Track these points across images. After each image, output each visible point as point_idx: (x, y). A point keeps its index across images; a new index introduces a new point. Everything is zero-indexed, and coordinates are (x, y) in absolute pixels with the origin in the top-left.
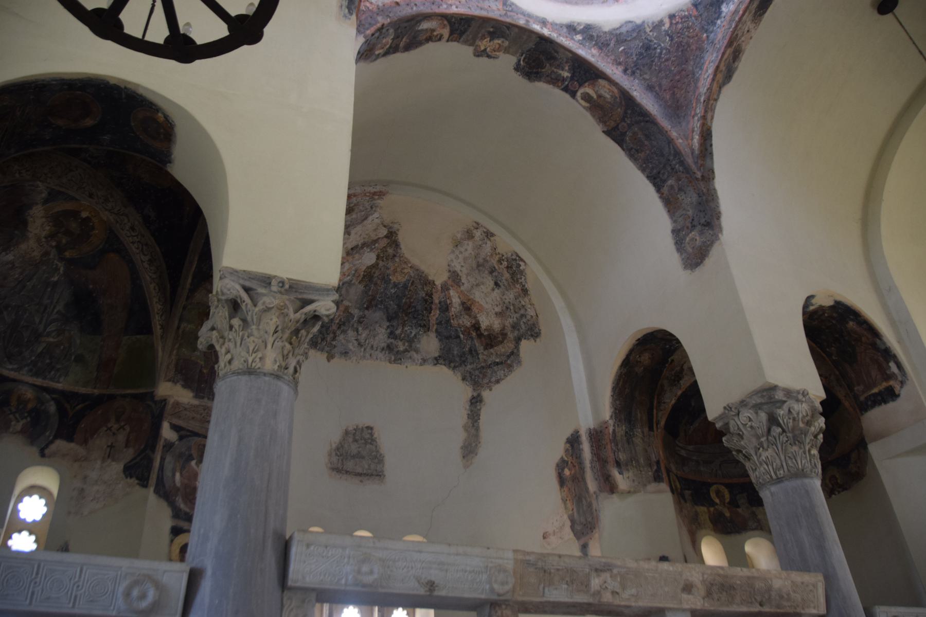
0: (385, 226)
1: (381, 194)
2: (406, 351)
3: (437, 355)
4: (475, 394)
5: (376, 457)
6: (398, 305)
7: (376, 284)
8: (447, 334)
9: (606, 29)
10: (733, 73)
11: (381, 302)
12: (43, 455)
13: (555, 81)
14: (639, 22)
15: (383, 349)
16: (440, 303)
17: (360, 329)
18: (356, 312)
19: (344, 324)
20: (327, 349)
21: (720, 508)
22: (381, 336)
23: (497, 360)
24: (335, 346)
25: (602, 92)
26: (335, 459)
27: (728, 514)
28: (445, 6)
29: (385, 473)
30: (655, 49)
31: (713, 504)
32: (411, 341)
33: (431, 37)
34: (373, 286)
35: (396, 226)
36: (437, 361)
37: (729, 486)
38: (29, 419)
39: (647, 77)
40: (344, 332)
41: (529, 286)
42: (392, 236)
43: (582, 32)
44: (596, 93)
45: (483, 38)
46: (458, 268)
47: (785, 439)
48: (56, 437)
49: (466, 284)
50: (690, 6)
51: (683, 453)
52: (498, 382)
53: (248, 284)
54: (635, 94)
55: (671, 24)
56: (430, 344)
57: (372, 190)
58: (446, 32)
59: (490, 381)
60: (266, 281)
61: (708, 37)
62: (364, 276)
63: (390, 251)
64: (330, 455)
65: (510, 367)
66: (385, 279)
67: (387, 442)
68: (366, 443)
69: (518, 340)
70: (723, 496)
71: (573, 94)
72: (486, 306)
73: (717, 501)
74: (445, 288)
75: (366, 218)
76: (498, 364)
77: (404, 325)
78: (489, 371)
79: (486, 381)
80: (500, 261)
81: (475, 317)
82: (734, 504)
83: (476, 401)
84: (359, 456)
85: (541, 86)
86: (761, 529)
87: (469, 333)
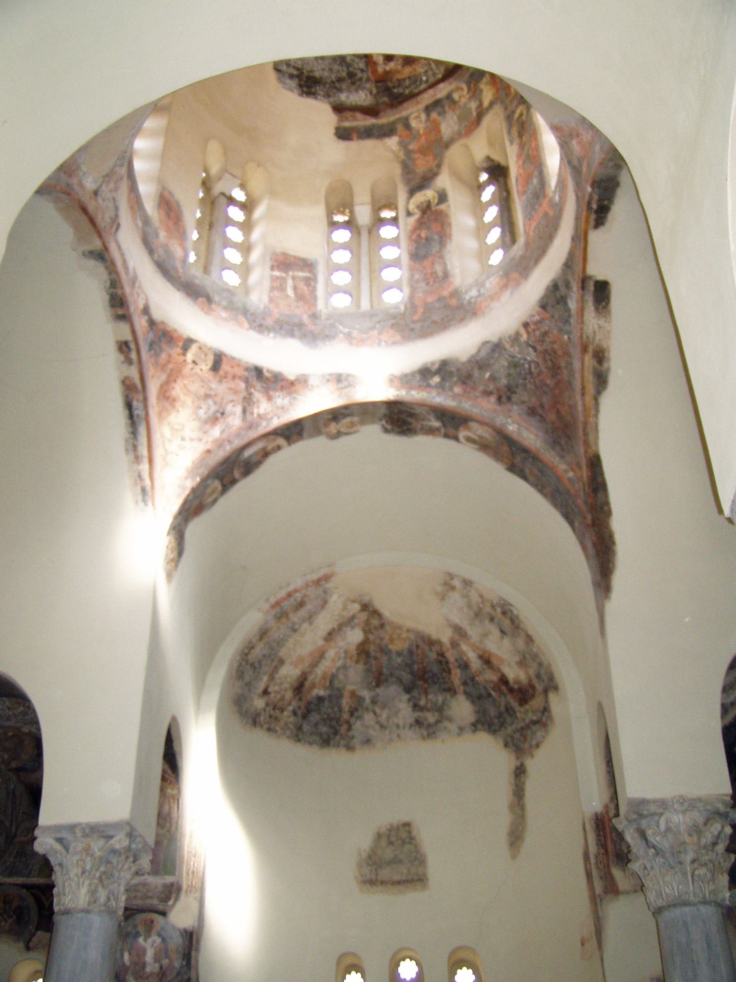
0: (354, 601)
1: (327, 578)
2: (438, 722)
3: (473, 719)
4: (519, 764)
5: (416, 858)
6: (412, 673)
7: (376, 658)
8: (478, 697)
9: (464, 358)
10: (606, 377)
11: (391, 675)
12: (28, 948)
13: (431, 431)
14: (495, 339)
15: (411, 726)
16: (456, 660)
17: (378, 710)
18: (366, 694)
19: (356, 709)
20: (342, 742)
22: (404, 711)
23: (535, 718)
24: (353, 737)
25: (480, 432)
26: (366, 870)
28: (264, 424)
29: (430, 876)
30: (523, 365)
32: (440, 709)
33: (265, 454)
34: (373, 662)
35: (366, 599)
36: (475, 726)
38: (14, 917)
39: (525, 398)
40: (359, 718)
41: (531, 632)
42: (365, 607)
43: (438, 372)
44: (475, 434)
45: (326, 425)
46: (457, 621)
47: (662, 860)
48: (37, 929)
49: (474, 633)
50: (539, 309)
52: (538, 746)
53: (59, 835)
54: (512, 428)
55: (528, 333)
56: (462, 709)
57: (315, 577)
58: (281, 441)
59: (531, 746)
60: (72, 828)
61: (569, 338)
62: (359, 654)
63: (375, 622)
64: (360, 866)
65: (545, 725)
66: (384, 650)
67: (429, 838)
68: (404, 842)
69: (546, 691)
71: (456, 439)
72: (504, 656)
74: (454, 645)
75: (325, 602)
76: (535, 723)
77: (426, 694)
78: (529, 732)
79: (527, 746)
80: (493, 607)
81: (499, 670)
83: (520, 772)
84: (395, 861)
85: (420, 440)
87: (500, 689)
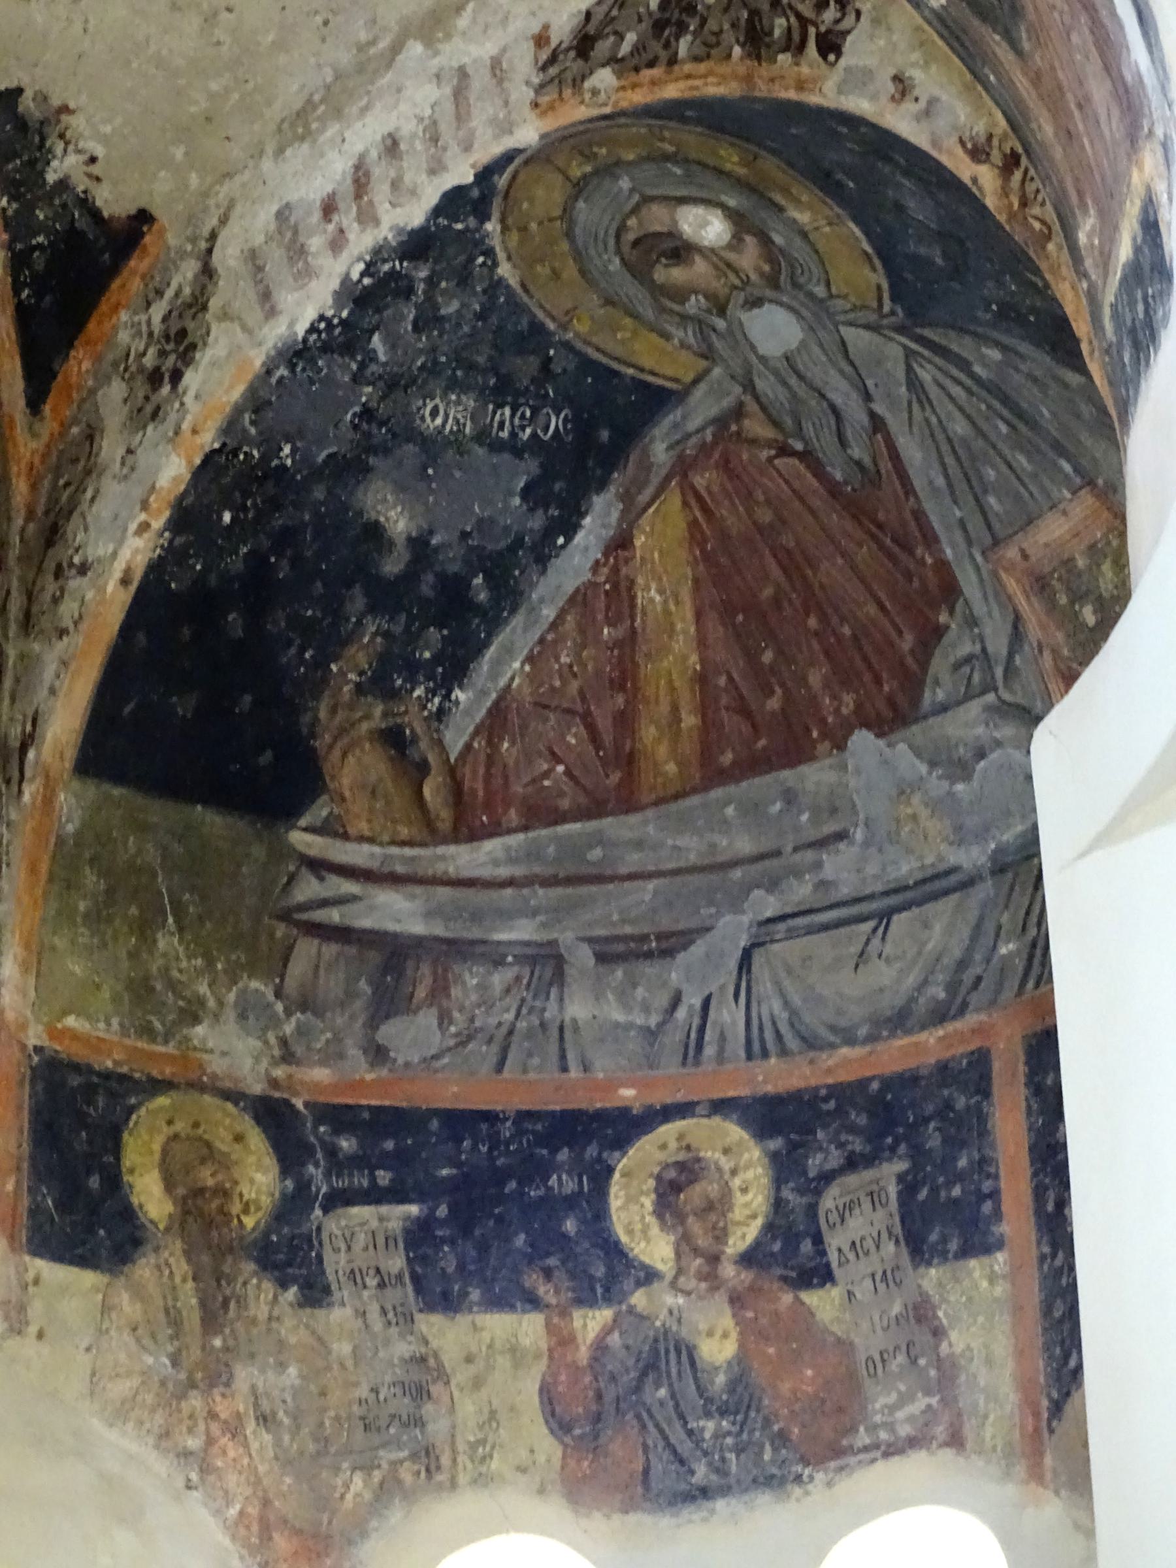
21: (656, 1303)
27: (718, 1348)
31: (608, 1271)
37: (770, 1116)
51: (396, 912)
70: (716, 1208)
73: (656, 1248)
82: (794, 1253)
86: (956, 1440)
